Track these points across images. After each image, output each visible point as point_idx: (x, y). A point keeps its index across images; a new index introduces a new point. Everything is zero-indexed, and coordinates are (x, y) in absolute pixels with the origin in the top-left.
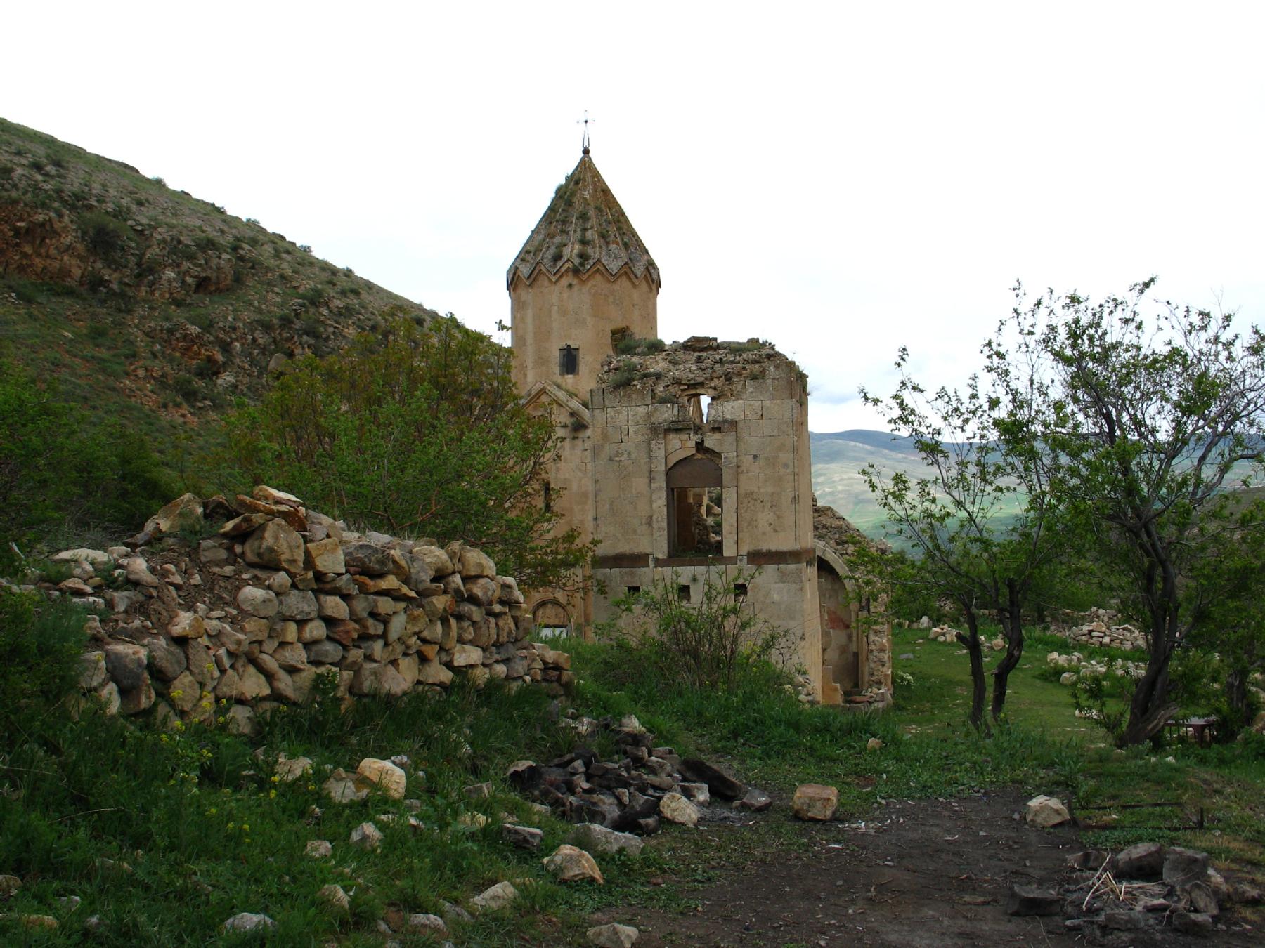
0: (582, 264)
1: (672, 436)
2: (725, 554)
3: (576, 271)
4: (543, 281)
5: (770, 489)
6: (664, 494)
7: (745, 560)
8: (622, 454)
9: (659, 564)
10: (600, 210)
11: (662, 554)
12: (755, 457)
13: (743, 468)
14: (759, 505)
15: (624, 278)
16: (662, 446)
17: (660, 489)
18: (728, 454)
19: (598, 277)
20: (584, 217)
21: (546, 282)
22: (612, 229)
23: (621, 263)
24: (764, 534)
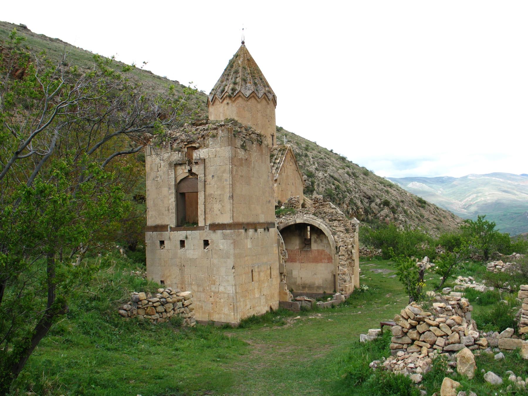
0: (233, 94)
1: (179, 168)
3: (230, 97)
4: (217, 102)
5: (219, 192)
6: (173, 196)
8: (158, 177)
9: (172, 229)
10: (245, 69)
11: (173, 225)
12: (213, 176)
13: (207, 182)
14: (214, 200)
15: (253, 98)
16: (173, 172)
17: (172, 193)
18: (201, 176)
19: (240, 99)
20: (236, 72)
21: (218, 103)
22: (249, 77)
23: (251, 92)
24: (216, 215)
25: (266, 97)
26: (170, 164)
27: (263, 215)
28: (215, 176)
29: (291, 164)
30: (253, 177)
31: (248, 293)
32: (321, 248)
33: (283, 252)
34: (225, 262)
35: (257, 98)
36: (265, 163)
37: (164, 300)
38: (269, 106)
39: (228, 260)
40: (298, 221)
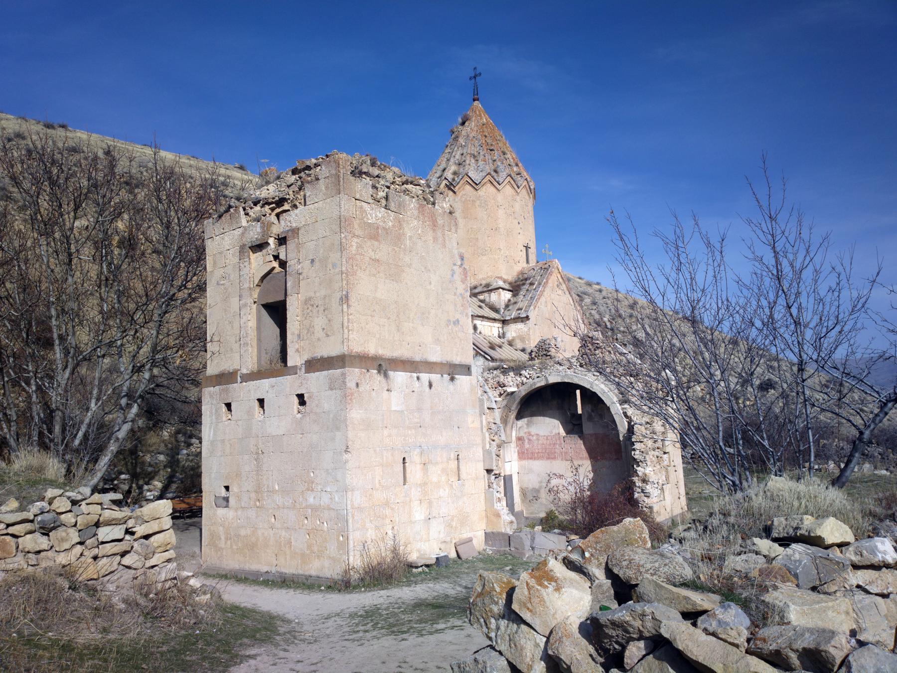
2: (290, 364)
5: (323, 292)
7: (303, 369)
12: (313, 261)
24: (319, 339)
26: (242, 247)
28: (317, 260)
29: (560, 292)
30: (410, 266)
31: (393, 509)
32: (600, 431)
33: (493, 426)
34: (333, 439)
35: (495, 183)
36: (444, 246)
37: (47, 517)
38: (518, 198)
39: (338, 434)
40: (553, 379)
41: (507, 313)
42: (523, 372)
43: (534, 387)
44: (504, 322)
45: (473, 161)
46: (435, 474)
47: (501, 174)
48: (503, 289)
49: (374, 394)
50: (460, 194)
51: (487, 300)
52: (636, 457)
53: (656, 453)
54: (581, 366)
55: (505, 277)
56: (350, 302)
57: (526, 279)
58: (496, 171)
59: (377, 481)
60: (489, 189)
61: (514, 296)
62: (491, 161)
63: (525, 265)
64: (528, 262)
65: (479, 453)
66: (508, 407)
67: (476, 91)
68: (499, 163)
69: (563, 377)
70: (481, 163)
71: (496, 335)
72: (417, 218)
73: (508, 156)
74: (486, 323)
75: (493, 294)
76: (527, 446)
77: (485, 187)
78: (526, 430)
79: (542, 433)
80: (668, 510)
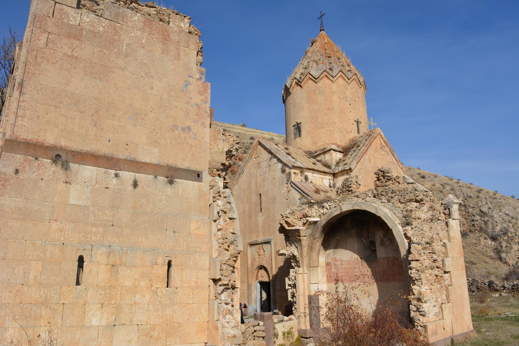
25: (344, 76)
27: (156, 150)
29: (383, 153)
41: (337, 168)
42: (325, 204)
43: (331, 216)
44: (334, 175)
45: (315, 64)
46: (127, 277)
47: (334, 71)
48: (335, 151)
49: (43, 184)
50: (305, 87)
51: (323, 160)
52: (412, 275)
53: (436, 272)
54: (374, 197)
55: (339, 143)
56: (24, 90)
57: (355, 144)
58: (331, 69)
59: (31, 276)
60: (326, 81)
61: (344, 156)
62: (327, 63)
63: (356, 135)
64: (358, 132)
65: (205, 261)
66: (312, 235)
67: (322, 25)
68: (334, 65)
69: (354, 205)
70: (320, 65)
71: (327, 184)
72: (143, 30)
73: (343, 60)
74: (317, 175)
75: (327, 154)
76: (334, 270)
77: (322, 80)
78: (333, 257)
79: (344, 259)
80: (448, 329)
